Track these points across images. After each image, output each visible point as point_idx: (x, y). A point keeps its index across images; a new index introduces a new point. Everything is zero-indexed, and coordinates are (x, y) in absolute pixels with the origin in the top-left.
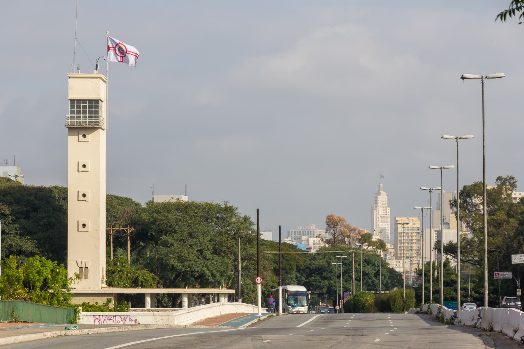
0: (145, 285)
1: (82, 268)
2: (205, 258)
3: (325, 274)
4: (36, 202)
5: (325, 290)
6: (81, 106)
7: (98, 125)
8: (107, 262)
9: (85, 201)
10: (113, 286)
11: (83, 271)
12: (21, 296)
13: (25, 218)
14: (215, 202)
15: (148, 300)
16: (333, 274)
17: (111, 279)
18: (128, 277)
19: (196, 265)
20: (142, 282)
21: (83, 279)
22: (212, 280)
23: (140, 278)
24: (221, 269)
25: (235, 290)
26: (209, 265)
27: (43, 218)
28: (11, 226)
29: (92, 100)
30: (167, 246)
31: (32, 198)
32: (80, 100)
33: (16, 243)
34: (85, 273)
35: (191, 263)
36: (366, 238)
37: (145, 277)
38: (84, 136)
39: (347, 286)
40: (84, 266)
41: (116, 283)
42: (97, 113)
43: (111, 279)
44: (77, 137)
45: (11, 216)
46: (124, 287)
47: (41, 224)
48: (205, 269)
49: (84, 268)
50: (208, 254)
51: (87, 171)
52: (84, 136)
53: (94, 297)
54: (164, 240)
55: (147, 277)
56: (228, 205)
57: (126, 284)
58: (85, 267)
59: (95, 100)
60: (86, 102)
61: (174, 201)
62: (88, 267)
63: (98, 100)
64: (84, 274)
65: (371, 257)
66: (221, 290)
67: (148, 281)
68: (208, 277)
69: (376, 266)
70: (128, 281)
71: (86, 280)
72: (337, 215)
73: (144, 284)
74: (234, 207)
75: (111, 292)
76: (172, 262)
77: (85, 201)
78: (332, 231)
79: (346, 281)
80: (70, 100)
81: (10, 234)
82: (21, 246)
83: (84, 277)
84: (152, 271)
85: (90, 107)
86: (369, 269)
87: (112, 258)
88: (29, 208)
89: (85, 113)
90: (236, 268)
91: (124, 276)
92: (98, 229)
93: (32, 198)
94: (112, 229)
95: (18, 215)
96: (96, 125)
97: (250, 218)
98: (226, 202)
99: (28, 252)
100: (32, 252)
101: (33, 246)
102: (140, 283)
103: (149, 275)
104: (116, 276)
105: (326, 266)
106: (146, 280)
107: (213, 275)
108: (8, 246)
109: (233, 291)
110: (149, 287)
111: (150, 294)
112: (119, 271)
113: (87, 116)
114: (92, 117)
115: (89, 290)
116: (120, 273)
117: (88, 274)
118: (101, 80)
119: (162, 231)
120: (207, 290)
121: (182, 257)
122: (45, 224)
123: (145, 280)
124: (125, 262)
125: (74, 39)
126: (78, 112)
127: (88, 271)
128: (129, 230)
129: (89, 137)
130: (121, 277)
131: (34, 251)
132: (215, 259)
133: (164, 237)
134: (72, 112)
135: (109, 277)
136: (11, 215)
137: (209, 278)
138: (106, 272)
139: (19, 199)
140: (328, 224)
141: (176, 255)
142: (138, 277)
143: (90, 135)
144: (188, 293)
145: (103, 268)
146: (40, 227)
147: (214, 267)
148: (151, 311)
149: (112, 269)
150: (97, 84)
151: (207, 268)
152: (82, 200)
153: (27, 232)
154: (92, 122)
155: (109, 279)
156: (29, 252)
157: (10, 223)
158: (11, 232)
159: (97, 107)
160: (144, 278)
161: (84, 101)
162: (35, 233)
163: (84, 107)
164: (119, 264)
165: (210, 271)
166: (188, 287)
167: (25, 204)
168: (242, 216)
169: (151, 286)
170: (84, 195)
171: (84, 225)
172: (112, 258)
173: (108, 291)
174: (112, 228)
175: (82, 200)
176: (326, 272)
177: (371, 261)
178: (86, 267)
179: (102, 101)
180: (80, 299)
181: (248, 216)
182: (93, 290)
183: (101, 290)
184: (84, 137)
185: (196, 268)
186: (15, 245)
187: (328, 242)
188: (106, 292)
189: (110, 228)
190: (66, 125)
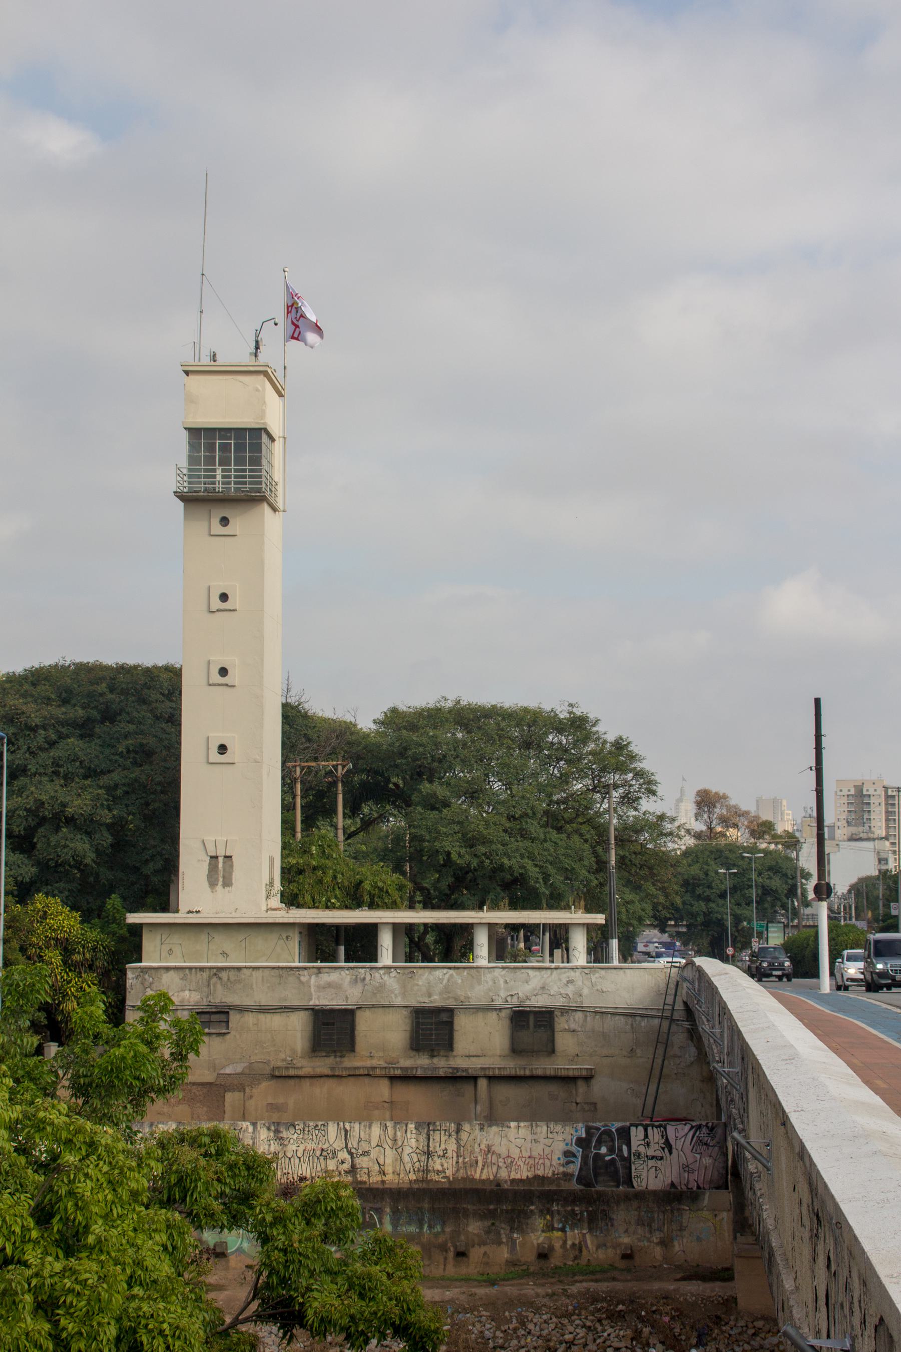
0: (380, 903)
1: (217, 857)
2: (523, 834)
3: (699, 891)
4: (110, 696)
5: (700, 919)
7: (259, 490)
8: (285, 846)
9: (227, 685)
10: (299, 906)
11: (221, 865)
12: (61, 933)
13: (82, 737)
14: (547, 707)
15: (386, 940)
16: (714, 890)
17: (294, 887)
18: (338, 883)
19: (506, 854)
20: (372, 897)
21: (219, 887)
22: (544, 889)
23: (367, 886)
24: (567, 863)
25: (603, 916)
26: (536, 853)
27: (126, 737)
28: (43, 755)
30: (433, 808)
31: (103, 687)
32: (214, 430)
33: (52, 798)
34: (224, 870)
35: (494, 847)
36: (763, 829)
37: (380, 884)
38: (225, 521)
39: (739, 912)
40: (221, 853)
41: (308, 898)
42: (256, 461)
43: (294, 887)
45: (45, 730)
46: (327, 907)
47: (120, 750)
48: (529, 864)
49: (221, 860)
50: (534, 827)
51: (230, 610)
52: (225, 521)
54: (428, 793)
55: (384, 883)
56: (578, 713)
57: (333, 901)
58: (226, 857)
59: (251, 430)
60: (229, 435)
61: (449, 704)
62: (231, 857)
63: (261, 429)
64: (221, 873)
65: (779, 861)
66: (573, 916)
67: (387, 892)
68: (536, 882)
69: (788, 877)
70: (337, 892)
71: (227, 889)
72: (715, 787)
73: (376, 899)
74: (592, 716)
75: (291, 921)
76: (446, 844)
77: (227, 685)
78: (706, 816)
79: (738, 904)
80: (190, 430)
81: (40, 774)
82: (64, 805)
84: (398, 868)
85: (240, 448)
86: (776, 883)
87: (299, 835)
88: (95, 714)
89: (224, 462)
90: (601, 865)
91: (328, 879)
92: (258, 757)
93: (103, 687)
94: (300, 765)
95: (64, 730)
96: (252, 490)
97: (629, 743)
98: (571, 705)
99: (82, 818)
100: (92, 819)
101: (96, 805)
102: (366, 898)
103: (390, 879)
104: (308, 880)
105: (702, 876)
106: (383, 891)
107: (546, 877)
108: (31, 804)
109: (599, 919)
110: (387, 908)
111: (391, 927)
112: (315, 869)
113: (233, 467)
114: (245, 471)
115: (234, 915)
116: (316, 871)
117: (231, 874)
118: (267, 382)
119: (420, 774)
120: (538, 916)
121: (470, 832)
122: (128, 751)
123: (381, 889)
124: (329, 846)
125: (200, 276)
126: (210, 461)
127: (232, 866)
128: (340, 768)
129: (238, 524)
130: (320, 882)
131: (98, 818)
132: (550, 839)
133: (426, 787)
134: (192, 460)
135: (290, 882)
136: (44, 728)
137: (538, 885)
138: (283, 869)
139: (69, 691)
140: (699, 804)
141: (457, 828)
142: (361, 882)
144: (489, 924)
145: (271, 860)
146: (117, 757)
147: (549, 858)
148: (392, 970)
149: (298, 863)
150: (258, 390)
151: (533, 860)
152: (219, 685)
153: (82, 771)
154: (245, 483)
155: (289, 888)
156: (85, 821)
157: (41, 749)
158: (42, 770)
159: (257, 448)
160: (375, 887)
161: (225, 432)
162: (103, 773)
163: (225, 448)
164: (316, 850)
165: (541, 867)
166: (491, 908)
167: (84, 703)
168: (611, 737)
169: (393, 906)
170: (223, 672)
171: (223, 749)
172: (299, 835)
173: (283, 917)
174: (298, 763)
175: (219, 685)
176: (701, 887)
177: (780, 868)
178: (227, 855)
179: (273, 440)
181: (624, 737)
182: (244, 915)
183: (266, 915)
185: (506, 861)
186: (48, 803)
187: (698, 836)
188: (277, 921)
189: (294, 764)
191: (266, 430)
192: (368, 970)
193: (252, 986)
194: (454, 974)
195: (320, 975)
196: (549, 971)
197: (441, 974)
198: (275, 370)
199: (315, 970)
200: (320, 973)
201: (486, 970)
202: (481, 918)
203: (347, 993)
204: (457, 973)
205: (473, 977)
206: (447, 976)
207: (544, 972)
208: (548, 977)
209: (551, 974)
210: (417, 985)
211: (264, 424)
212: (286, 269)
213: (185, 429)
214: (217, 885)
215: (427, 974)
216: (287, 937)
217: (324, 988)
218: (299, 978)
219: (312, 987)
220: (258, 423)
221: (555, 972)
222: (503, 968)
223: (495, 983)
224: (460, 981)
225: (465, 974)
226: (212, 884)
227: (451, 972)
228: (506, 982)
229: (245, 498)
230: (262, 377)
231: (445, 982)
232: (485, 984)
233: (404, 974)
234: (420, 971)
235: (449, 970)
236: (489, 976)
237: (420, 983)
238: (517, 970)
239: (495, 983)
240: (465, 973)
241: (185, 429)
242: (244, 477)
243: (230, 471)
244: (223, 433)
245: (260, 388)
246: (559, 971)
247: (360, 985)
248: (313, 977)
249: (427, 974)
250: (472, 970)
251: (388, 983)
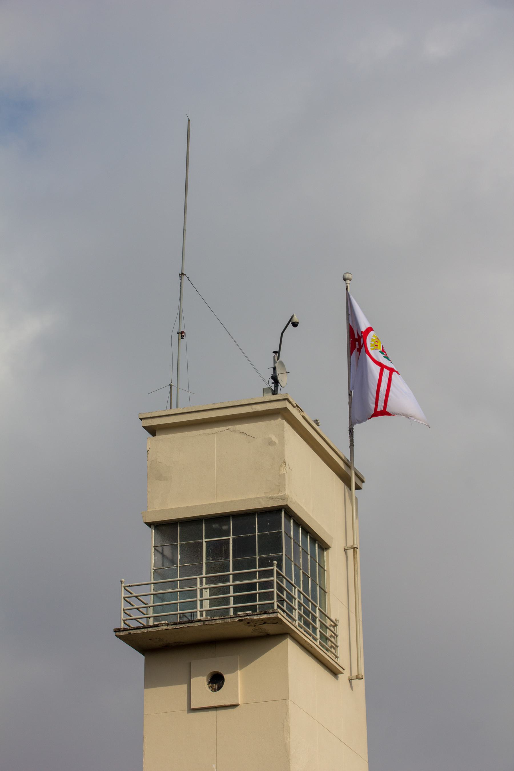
6: (204, 544)
29: (249, 514)
32: (196, 521)
44: (185, 687)
60: (225, 528)
63: (276, 511)
118: (287, 427)
125: (178, 277)
143: (239, 672)
150: (271, 443)
184: (215, 686)
190: (123, 626)
191: (290, 514)
198: (316, 422)
211: (282, 498)
212: (347, 276)
213: (149, 524)
220: (272, 498)
229: (249, 631)
230: (280, 422)
241: (149, 524)
242: (252, 598)
243: (226, 590)
244: (215, 526)
245: (274, 439)
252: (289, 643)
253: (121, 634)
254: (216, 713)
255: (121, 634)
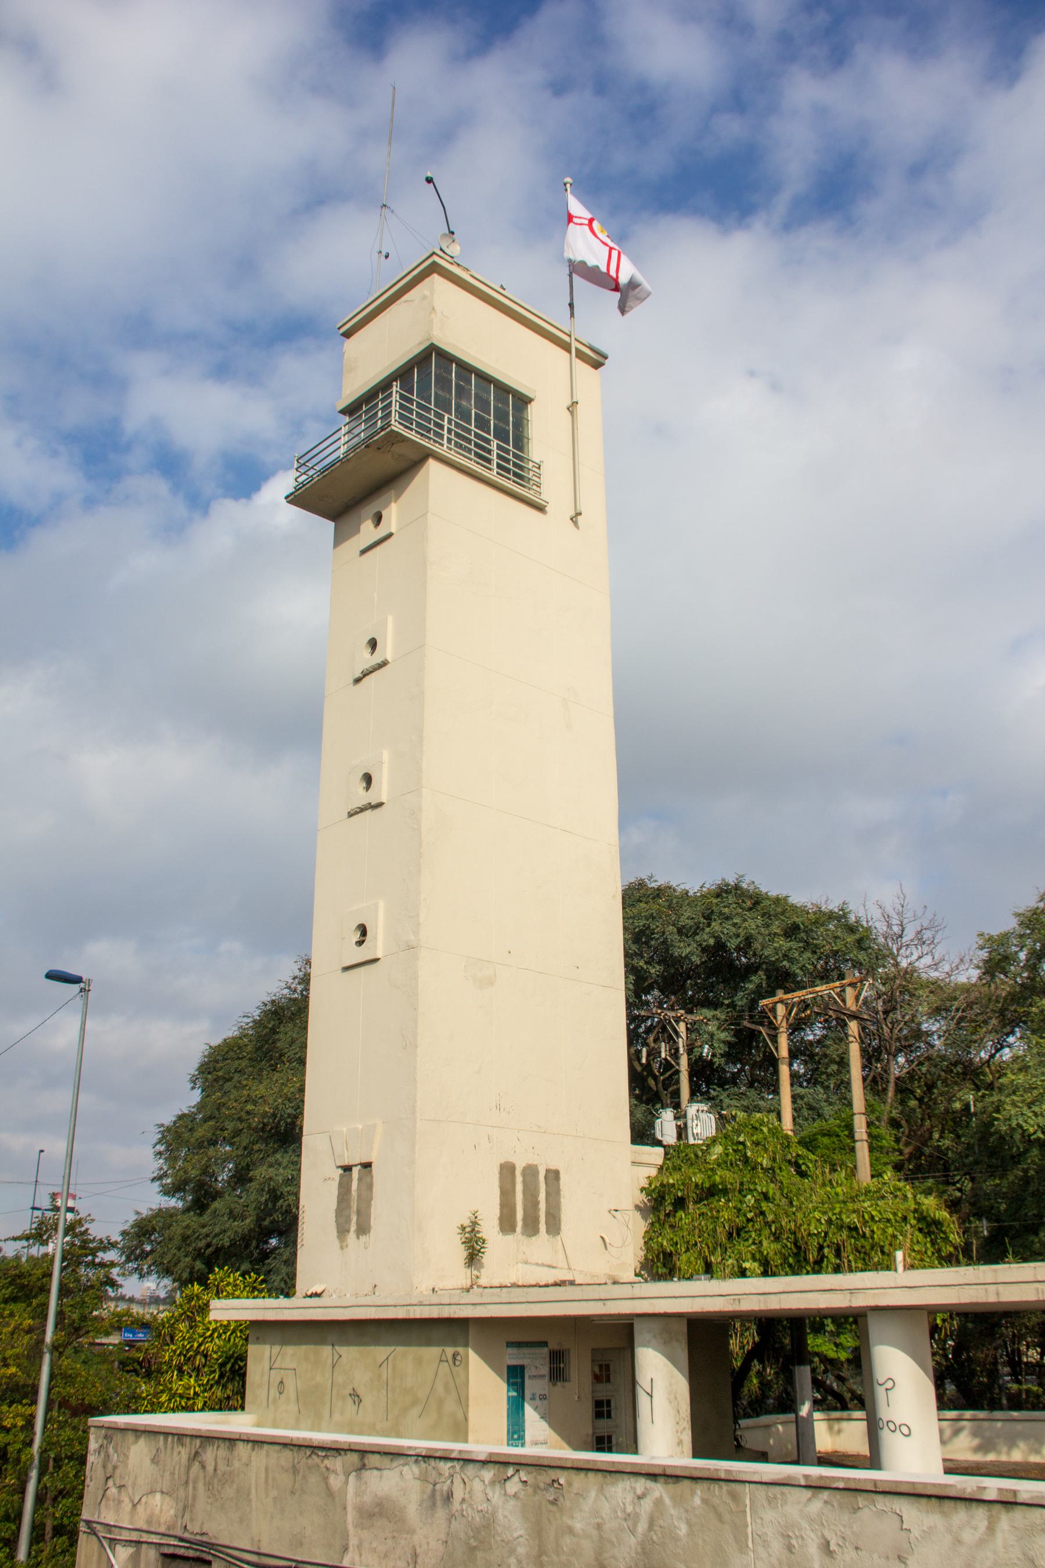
21: (352, 1235)
34: (359, 1196)
49: (356, 1171)
53: (390, 1349)
71: (363, 1238)
83: (353, 1227)
92: (412, 937)
111: (683, 1327)
127: (370, 1187)
148: (510, 1471)
180: (336, 1357)
192: (458, 1466)
193: (249, 1494)
194: (667, 1500)
195: (366, 1474)
196: (980, 1514)
197: (629, 1497)
198: (502, 287)
199: (354, 1458)
200: (363, 1467)
201: (761, 1492)
202: (852, 1291)
203: (416, 1539)
204: (673, 1498)
205: (720, 1518)
206: (647, 1505)
207: (960, 1515)
208: (981, 1543)
209: (991, 1529)
210: (571, 1531)
214: (348, 1231)
215: (593, 1494)
216: (455, 1356)
217: (371, 1515)
218: (326, 1479)
219: (349, 1509)
221: (1006, 1520)
222: (815, 1487)
223: (790, 1548)
224: (683, 1530)
225: (697, 1501)
226: (342, 1231)
227: (658, 1489)
228: (826, 1547)
230: (435, 277)
231: (642, 1527)
232: (760, 1550)
233: (536, 1488)
234: (579, 1481)
235: (650, 1484)
236: (769, 1515)
237: (578, 1526)
238: (861, 1500)
239: (790, 1548)
240: (697, 1495)
246: (1018, 1513)
247: (441, 1513)
248: (352, 1478)
249: (593, 1494)
250: (715, 1487)
251: (500, 1515)
252: (431, 463)
253: (290, 498)
254: (378, 549)
255: (290, 498)
